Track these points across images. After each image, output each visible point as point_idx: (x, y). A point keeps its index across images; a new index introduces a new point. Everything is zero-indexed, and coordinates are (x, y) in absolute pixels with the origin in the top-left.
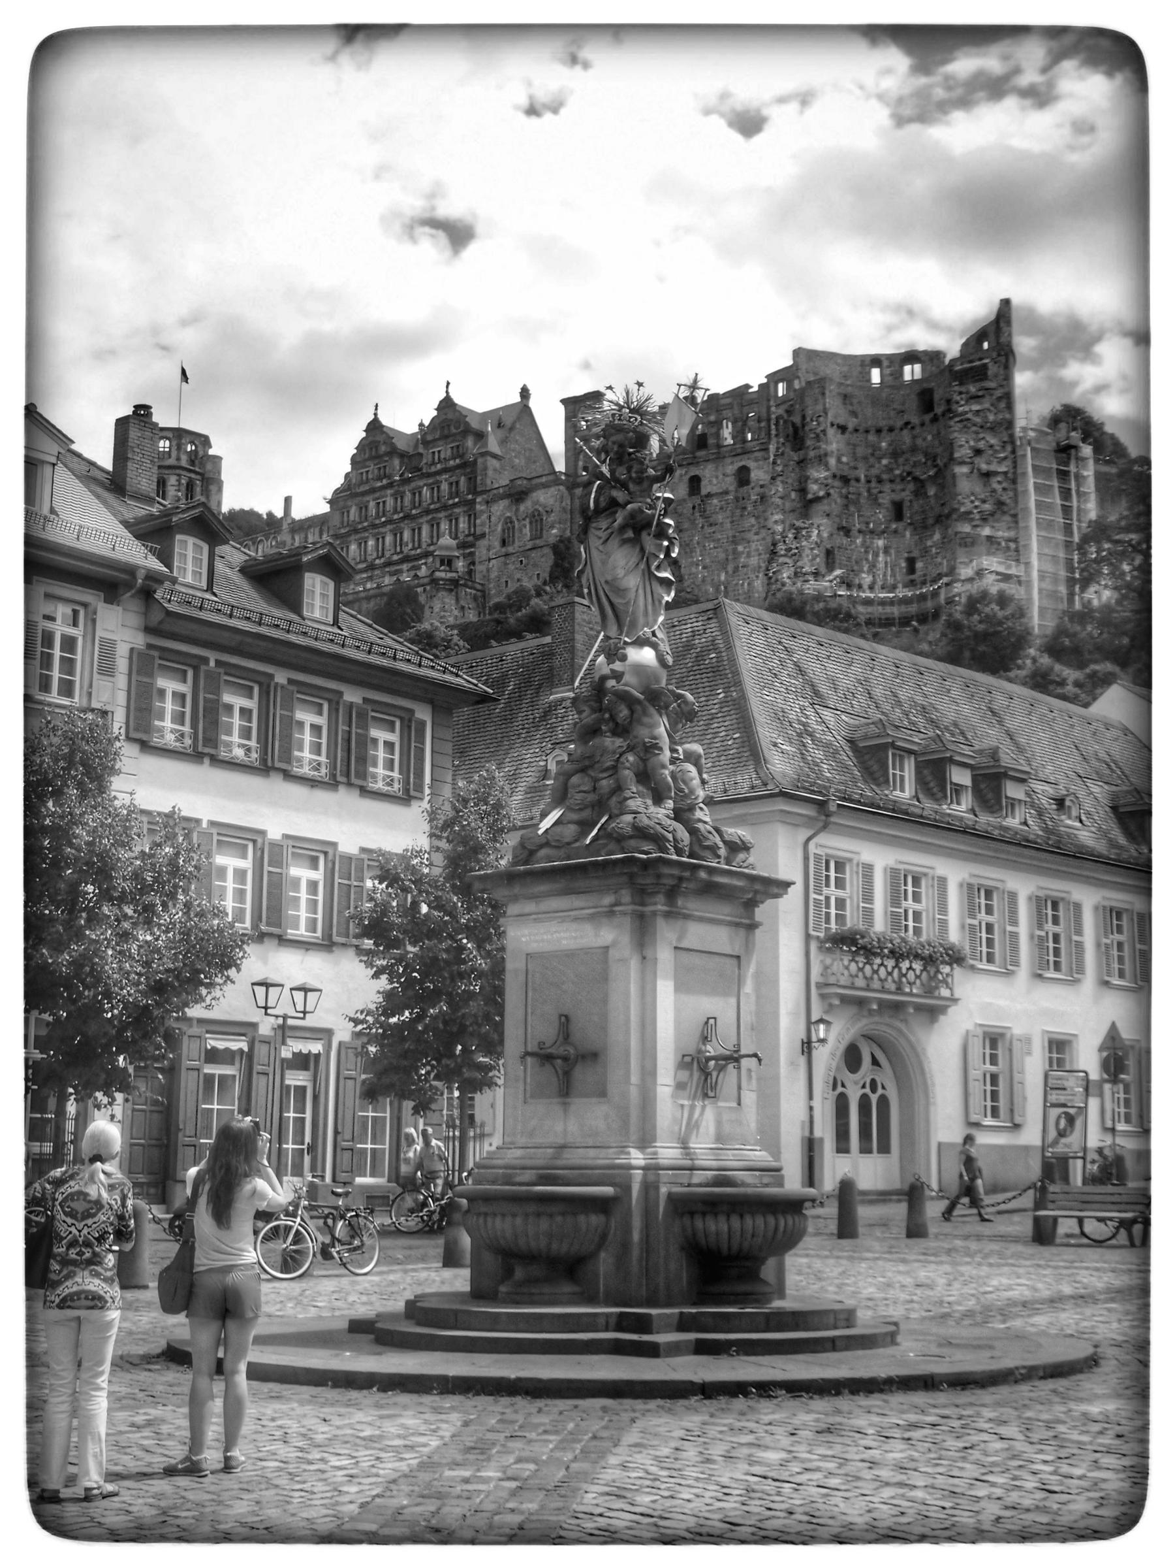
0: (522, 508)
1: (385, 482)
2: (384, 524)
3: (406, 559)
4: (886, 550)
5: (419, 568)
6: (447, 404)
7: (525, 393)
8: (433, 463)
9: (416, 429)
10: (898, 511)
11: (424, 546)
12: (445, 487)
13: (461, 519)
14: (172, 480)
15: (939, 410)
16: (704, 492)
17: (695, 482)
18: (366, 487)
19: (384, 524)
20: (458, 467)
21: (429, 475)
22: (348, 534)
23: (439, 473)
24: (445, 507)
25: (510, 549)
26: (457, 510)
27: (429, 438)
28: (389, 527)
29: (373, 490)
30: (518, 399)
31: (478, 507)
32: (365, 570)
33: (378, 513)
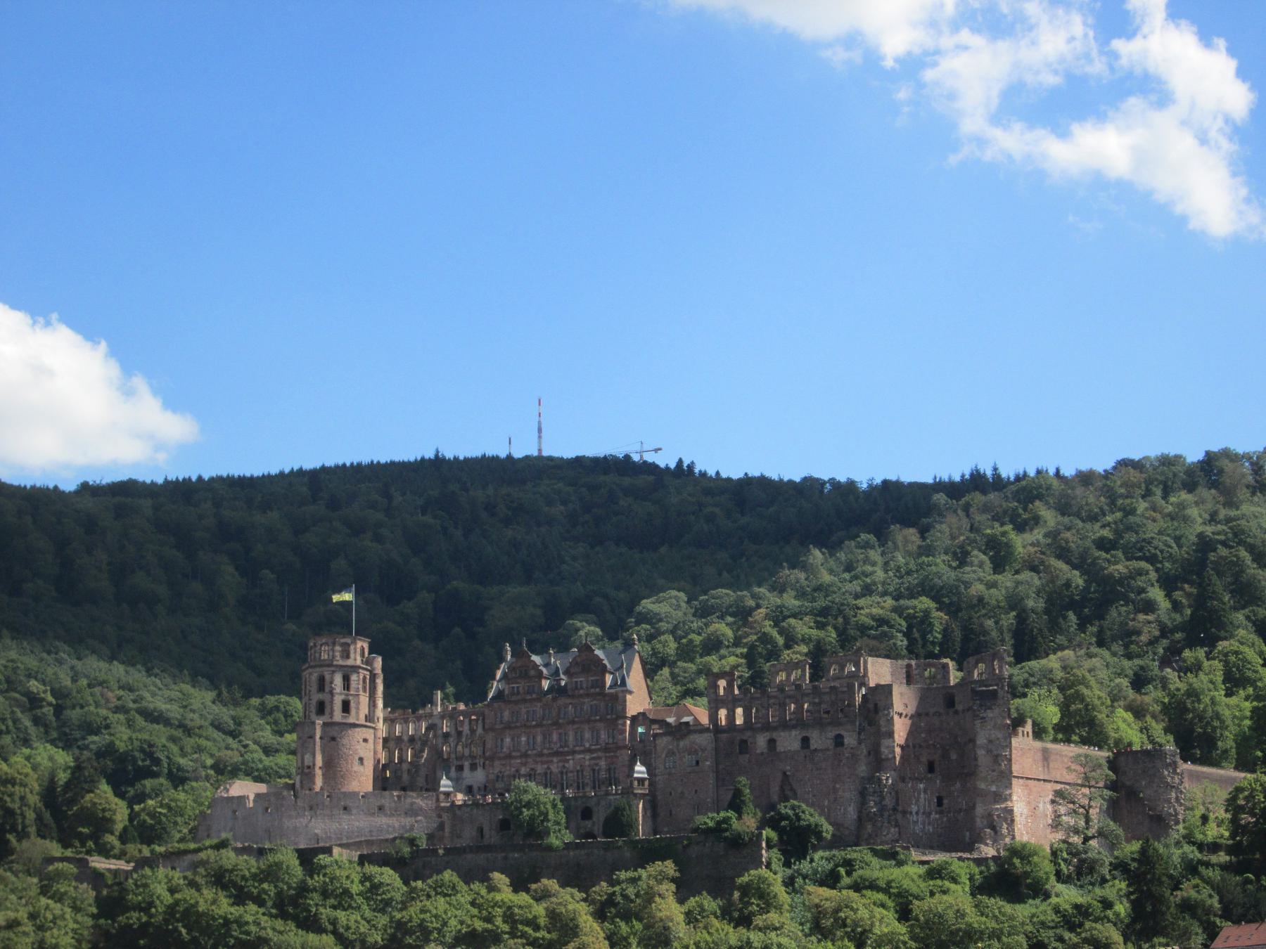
0: (682, 744)
4: (925, 792)
5: (567, 761)
10: (931, 768)
14: (354, 677)
15: (959, 707)
16: (812, 747)
17: (805, 741)
18: (519, 697)
20: (600, 694)
21: (573, 696)
23: (581, 696)
24: (589, 721)
27: (572, 670)
29: (525, 701)
32: (521, 757)
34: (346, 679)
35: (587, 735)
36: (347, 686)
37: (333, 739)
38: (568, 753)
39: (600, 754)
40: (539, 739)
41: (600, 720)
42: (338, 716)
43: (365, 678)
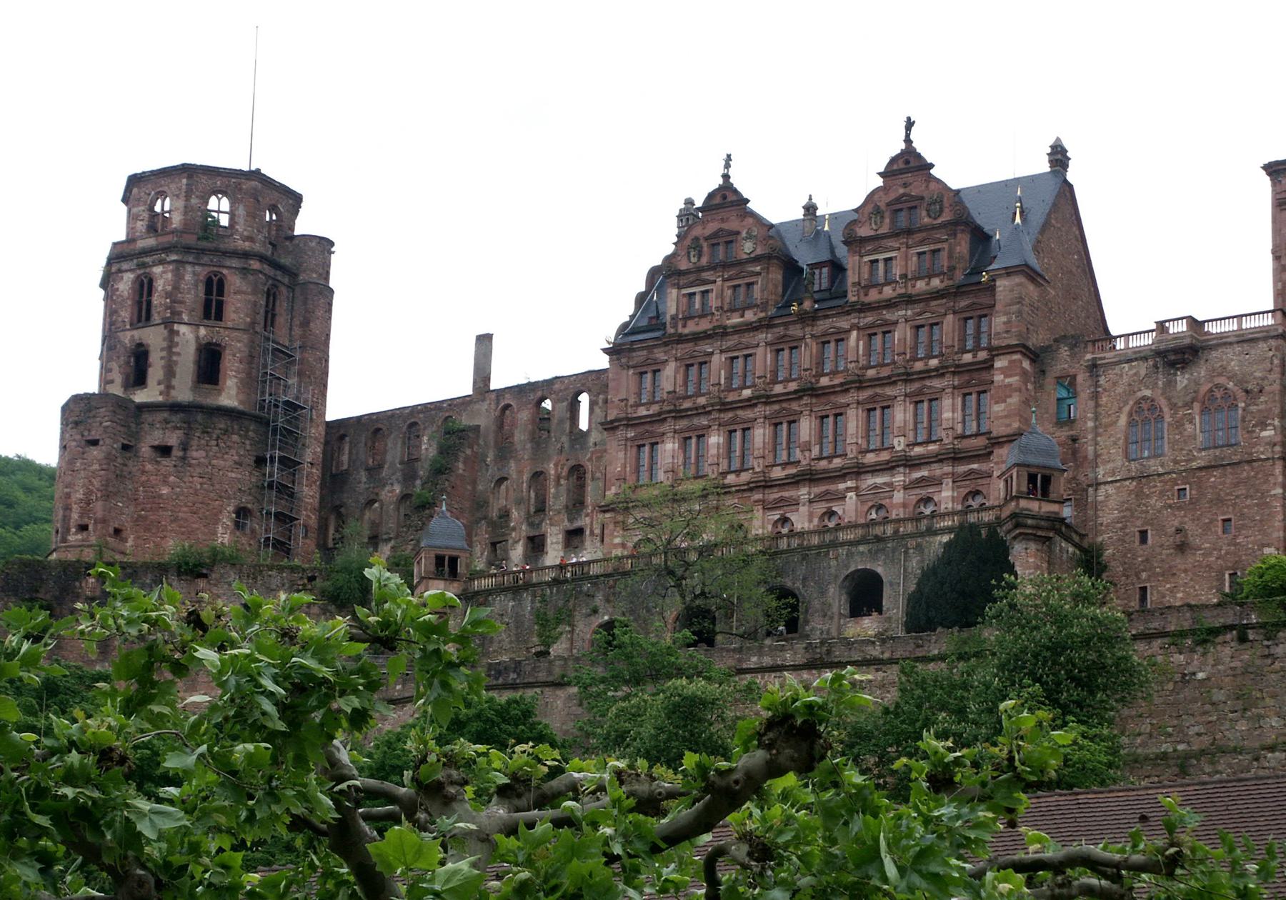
0: (1182, 380)
1: (750, 316)
2: (750, 403)
3: (809, 477)
6: (908, 166)
7: (1059, 157)
8: (872, 285)
9: (799, 214)
11: (852, 452)
12: (902, 334)
13: (947, 402)
18: (705, 325)
19: (750, 403)
20: (938, 295)
21: (864, 308)
22: (659, 419)
23: (890, 304)
24: (908, 377)
25: (1154, 466)
26: (936, 383)
27: (864, 232)
28: (759, 410)
29: (721, 333)
30: (1044, 167)
31: (998, 378)
33: (729, 378)
34: (214, 291)
35: (901, 414)
36: (213, 309)
37: (165, 451)
38: (842, 475)
39: (938, 470)
40: (760, 435)
41: (939, 373)
42: (184, 392)
43: (271, 295)
